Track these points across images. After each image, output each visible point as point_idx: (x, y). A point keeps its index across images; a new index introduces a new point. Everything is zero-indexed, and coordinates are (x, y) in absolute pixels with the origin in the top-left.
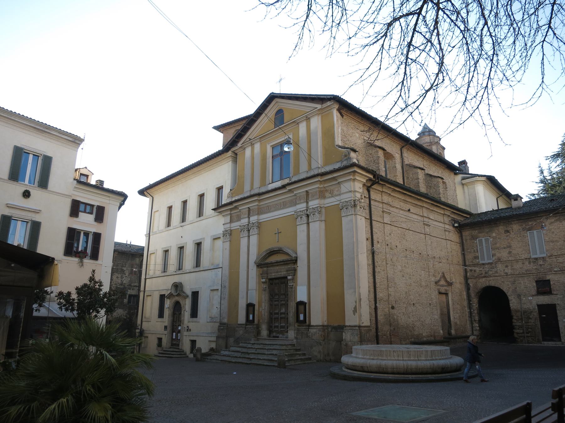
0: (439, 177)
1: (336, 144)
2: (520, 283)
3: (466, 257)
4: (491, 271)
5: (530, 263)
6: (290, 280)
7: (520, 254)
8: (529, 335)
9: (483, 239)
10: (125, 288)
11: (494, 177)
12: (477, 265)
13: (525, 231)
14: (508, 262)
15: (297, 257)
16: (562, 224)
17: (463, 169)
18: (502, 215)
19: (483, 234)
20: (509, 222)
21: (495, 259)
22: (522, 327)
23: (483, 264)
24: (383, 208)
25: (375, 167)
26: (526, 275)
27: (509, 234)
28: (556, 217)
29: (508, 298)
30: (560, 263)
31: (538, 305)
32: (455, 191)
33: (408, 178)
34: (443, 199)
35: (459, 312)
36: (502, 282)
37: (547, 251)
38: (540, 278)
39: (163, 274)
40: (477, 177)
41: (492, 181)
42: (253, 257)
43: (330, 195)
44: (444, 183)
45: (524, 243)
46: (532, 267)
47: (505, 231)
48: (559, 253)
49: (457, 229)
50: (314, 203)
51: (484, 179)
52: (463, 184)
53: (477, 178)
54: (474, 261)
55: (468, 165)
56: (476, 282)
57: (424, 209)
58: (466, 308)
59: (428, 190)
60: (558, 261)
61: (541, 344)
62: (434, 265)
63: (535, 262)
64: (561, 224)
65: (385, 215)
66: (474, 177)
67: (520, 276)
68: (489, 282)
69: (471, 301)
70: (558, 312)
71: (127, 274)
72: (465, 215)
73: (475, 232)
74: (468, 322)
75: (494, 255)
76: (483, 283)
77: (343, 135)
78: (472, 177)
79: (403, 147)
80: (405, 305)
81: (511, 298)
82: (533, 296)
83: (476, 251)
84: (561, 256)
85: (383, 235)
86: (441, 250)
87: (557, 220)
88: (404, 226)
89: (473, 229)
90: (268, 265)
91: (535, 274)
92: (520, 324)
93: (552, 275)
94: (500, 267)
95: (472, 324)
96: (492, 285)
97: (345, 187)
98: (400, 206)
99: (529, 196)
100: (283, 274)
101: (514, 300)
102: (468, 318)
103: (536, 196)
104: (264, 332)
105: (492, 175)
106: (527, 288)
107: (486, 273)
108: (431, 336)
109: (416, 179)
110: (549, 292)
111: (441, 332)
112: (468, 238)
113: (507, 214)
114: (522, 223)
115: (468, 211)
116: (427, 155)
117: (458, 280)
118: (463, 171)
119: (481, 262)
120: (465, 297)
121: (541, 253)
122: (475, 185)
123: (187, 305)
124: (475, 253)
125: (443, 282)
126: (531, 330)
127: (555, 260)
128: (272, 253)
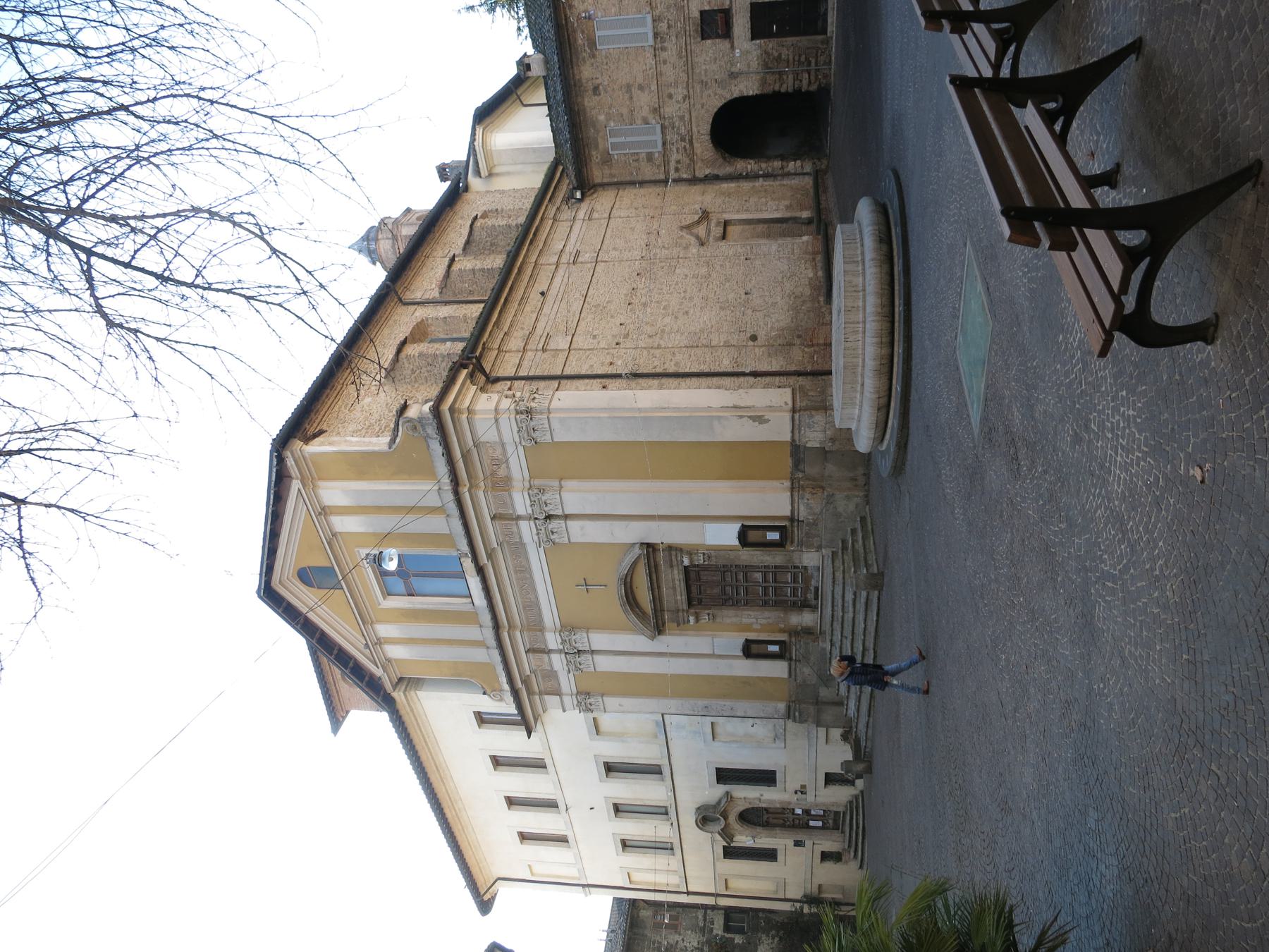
0: (471, 226)
1: (385, 448)
2: (706, 71)
3: (647, 178)
4: (678, 128)
5: (664, 49)
6: (691, 560)
7: (644, 68)
8: (813, 61)
9: (611, 140)
10: (708, 942)
11: (478, 109)
12: (665, 156)
14: (660, 93)
15: (642, 544)
17: (455, 172)
18: (560, 97)
19: (600, 140)
20: (575, 85)
21: (654, 118)
22: (798, 74)
23: (664, 144)
24: (536, 350)
25: (444, 364)
26: (689, 59)
27: (601, 87)
29: (736, 99)
31: (753, 38)
32: (502, 192)
33: (471, 293)
34: (522, 220)
35: (764, 200)
36: (702, 107)
37: (640, 12)
38: (696, 31)
39: (677, 851)
40: (476, 143)
41: (486, 114)
42: (640, 642)
43: (504, 466)
44: (485, 215)
46: (672, 45)
47: (595, 94)
49: (589, 193)
50: (521, 504)
51: (479, 131)
52: (490, 175)
53: (478, 143)
55: (447, 161)
56: (702, 160)
57: (542, 261)
58: (757, 184)
59: (499, 249)
61: (832, 38)
62: (664, 247)
63: (662, 38)
65: (552, 346)
66: (475, 150)
69: (740, 174)
71: (677, 938)
72: (558, 175)
73: (596, 156)
74: (785, 182)
75: (646, 122)
76: (703, 146)
77: (367, 432)
78: (475, 155)
79: (400, 300)
80: (749, 312)
82: (732, 47)
83: (637, 158)
85: (595, 352)
86: (633, 229)
88: (576, 306)
89: (588, 161)
91: (688, 39)
92: (791, 77)
93: (690, 4)
94: (670, 110)
95: (788, 174)
96: (709, 127)
97: (486, 431)
100: (678, 575)
101: (742, 86)
102: (778, 183)
106: (715, 59)
107: (683, 140)
108: (814, 259)
109: (474, 274)
110: (726, 14)
111: (805, 238)
112: (607, 171)
113: (559, 88)
114: (578, 58)
115: (549, 169)
116: (422, 249)
117: (698, 198)
118: (460, 173)
119: (660, 148)
120: (733, 185)
121: (644, 25)
122: (493, 149)
123: (747, 794)
124: (641, 160)
125: (701, 230)
126: (804, 56)
128: (630, 599)
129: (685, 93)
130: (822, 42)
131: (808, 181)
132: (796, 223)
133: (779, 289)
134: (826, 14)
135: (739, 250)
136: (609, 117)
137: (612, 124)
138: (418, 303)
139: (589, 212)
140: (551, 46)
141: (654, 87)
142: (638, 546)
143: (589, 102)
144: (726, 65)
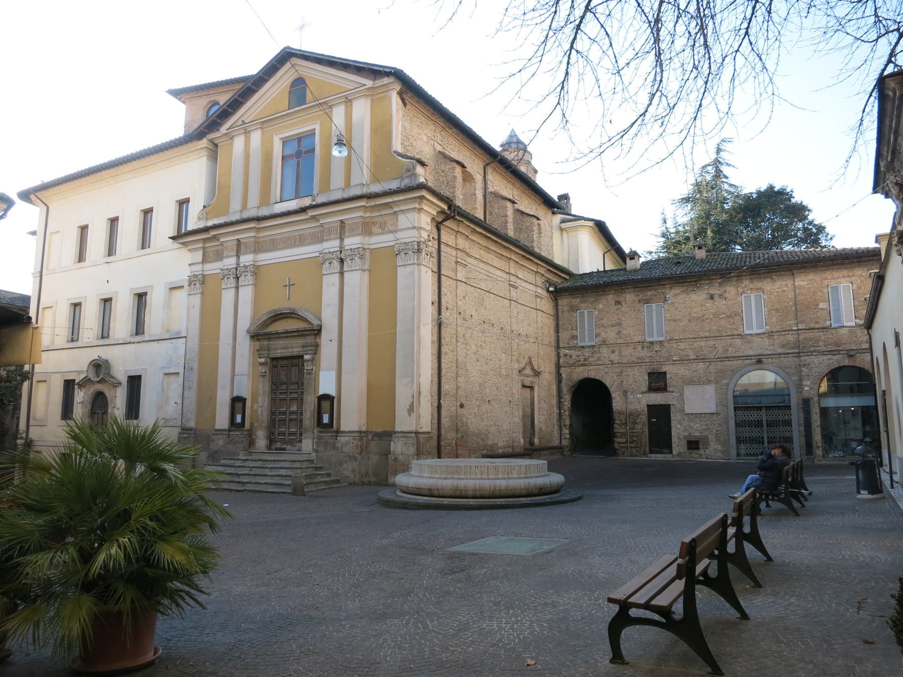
0: (533, 216)
2: (629, 375)
4: (592, 357)
5: (643, 348)
6: (308, 361)
7: (632, 335)
8: (633, 445)
9: (586, 312)
11: (604, 223)
12: (575, 348)
13: (642, 304)
16: (689, 298)
17: (564, 205)
18: (615, 279)
19: (586, 304)
20: (622, 289)
21: (599, 341)
22: (625, 435)
23: (583, 347)
26: (636, 365)
28: (683, 286)
30: (681, 350)
31: (648, 406)
32: (552, 238)
33: (491, 213)
34: (537, 250)
35: (546, 413)
36: (606, 373)
37: (666, 333)
38: (654, 369)
40: (583, 221)
41: (601, 228)
42: (245, 322)
43: (380, 231)
44: (539, 225)
45: (639, 320)
46: (645, 353)
47: (616, 302)
48: (681, 337)
49: (552, 296)
50: (352, 242)
51: (591, 224)
52: (562, 230)
53: (582, 222)
54: (571, 342)
56: (571, 372)
57: (512, 263)
58: (555, 408)
59: (517, 234)
60: (679, 347)
61: (647, 457)
63: (650, 347)
64: (688, 297)
65: (459, 268)
66: (578, 220)
67: (629, 365)
68: (588, 372)
69: (561, 398)
70: (672, 415)
72: (563, 276)
73: (576, 301)
74: (556, 427)
76: (580, 373)
78: (575, 220)
79: (487, 165)
80: (478, 403)
81: (615, 396)
82: (643, 393)
83: (574, 328)
84: (683, 341)
87: (682, 292)
88: (483, 285)
89: (573, 296)
90: (270, 336)
91: (649, 364)
92: (623, 431)
94: (604, 350)
95: (561, 430)
96: (592, 377)
98: (480, 255)
99: (645, 253)
100: (296, 351)
101: (618, 398)
102: (555, 423)
103: (653, 254)
104: (261, 442)
105: (602, 220)
106: (636, 382)
107: (585, 360)
110: (663, 389)
111: (522, 441)
112: (566, 308)
113: (620, 278)
115: (564, 268)
116: (518, 181)
118: (564, 210)
119: (580, 344)
120: (555, 392)
121: (658, 336)
122: (579, 233)
125: (528, 371)
126: (636, 439)
127: (675, 345)
128: (278, 316)
129: (615, 362)
130: (645, 451)
131: (556, 443)
132: (531, 435)
133: (491, 423)
134: (662, 453)
135: (516, 397)
136: (600, 311)
137: (596, 313)
138: (485, 177)
139: (540, 295)
140: (646, 274)
141: (619, 341)
142: (319, 323)
143: (611, 298)
144: (632, 389)
